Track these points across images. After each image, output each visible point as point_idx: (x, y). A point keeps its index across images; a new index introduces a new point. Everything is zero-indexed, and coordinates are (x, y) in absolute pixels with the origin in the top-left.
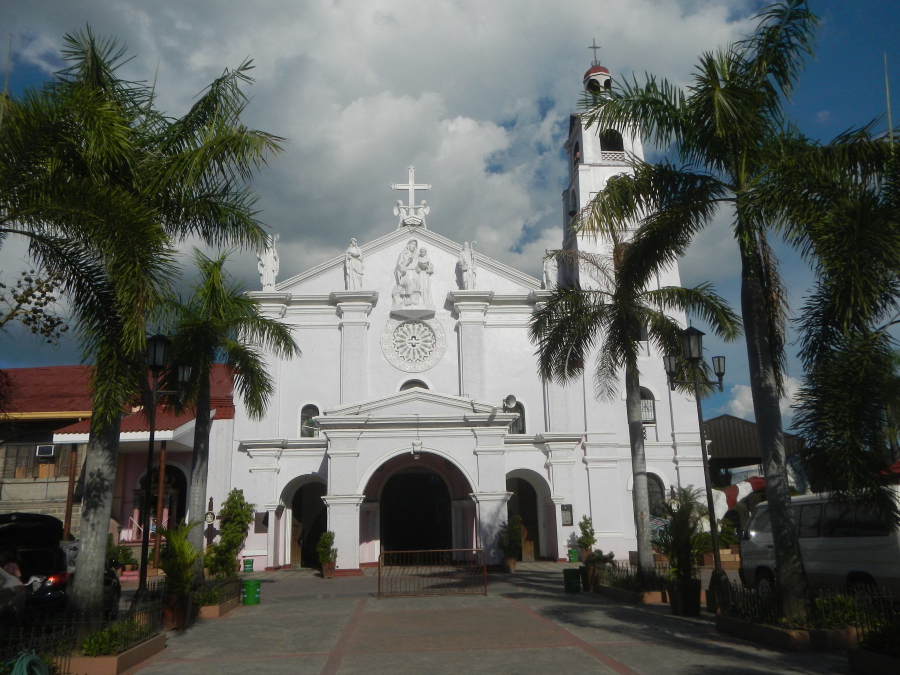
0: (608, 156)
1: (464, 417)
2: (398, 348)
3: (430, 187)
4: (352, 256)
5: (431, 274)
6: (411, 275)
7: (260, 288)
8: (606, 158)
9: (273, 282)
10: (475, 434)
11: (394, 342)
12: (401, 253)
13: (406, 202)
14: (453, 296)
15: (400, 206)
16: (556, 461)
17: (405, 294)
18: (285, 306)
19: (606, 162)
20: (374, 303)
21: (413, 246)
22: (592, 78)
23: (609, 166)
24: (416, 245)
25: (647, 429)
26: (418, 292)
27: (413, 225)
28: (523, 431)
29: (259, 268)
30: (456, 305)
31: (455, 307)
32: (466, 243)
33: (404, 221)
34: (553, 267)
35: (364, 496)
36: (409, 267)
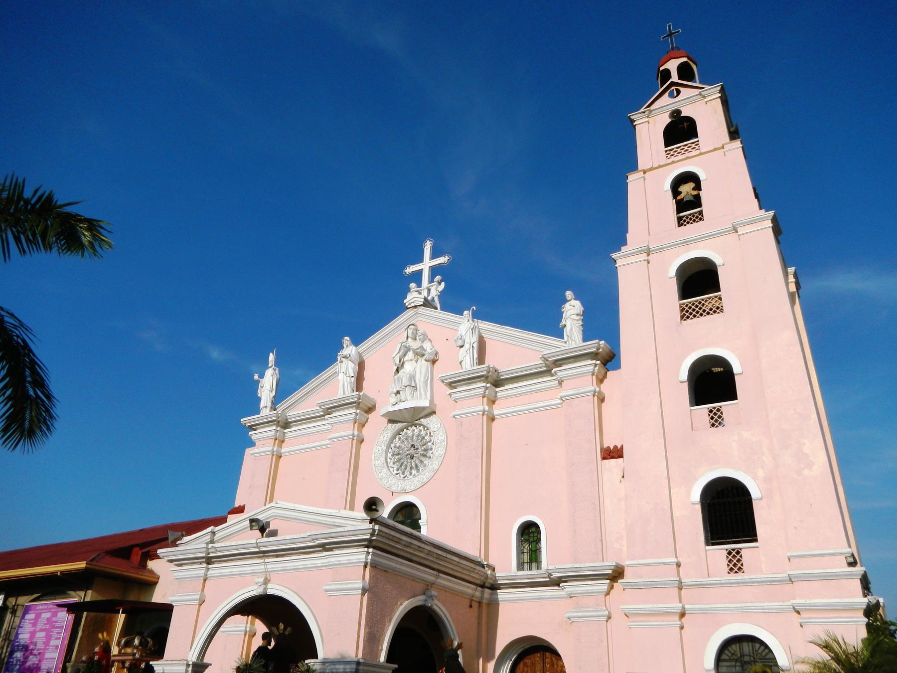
0: (675, 151)
2: (394, 464)
3: (447, 258)
4: (343, 357)
5: (434, 362)
6: (408, 367)
8: (672, 155)
9: (269, 404)
11: (390, 455)
13: (419, 285)
16: (575, 614)
17: (395, 391)
18: (279, 429)
19: (673, 159)
20: (370, 410)
21: (410, 331)
22: (661, 69)
23: (673, 162)
25: (743, 552)
26: (408, 385)
27: (415, 307)
28: (539, 567)
34: (575, 317)
36: (406, 358)
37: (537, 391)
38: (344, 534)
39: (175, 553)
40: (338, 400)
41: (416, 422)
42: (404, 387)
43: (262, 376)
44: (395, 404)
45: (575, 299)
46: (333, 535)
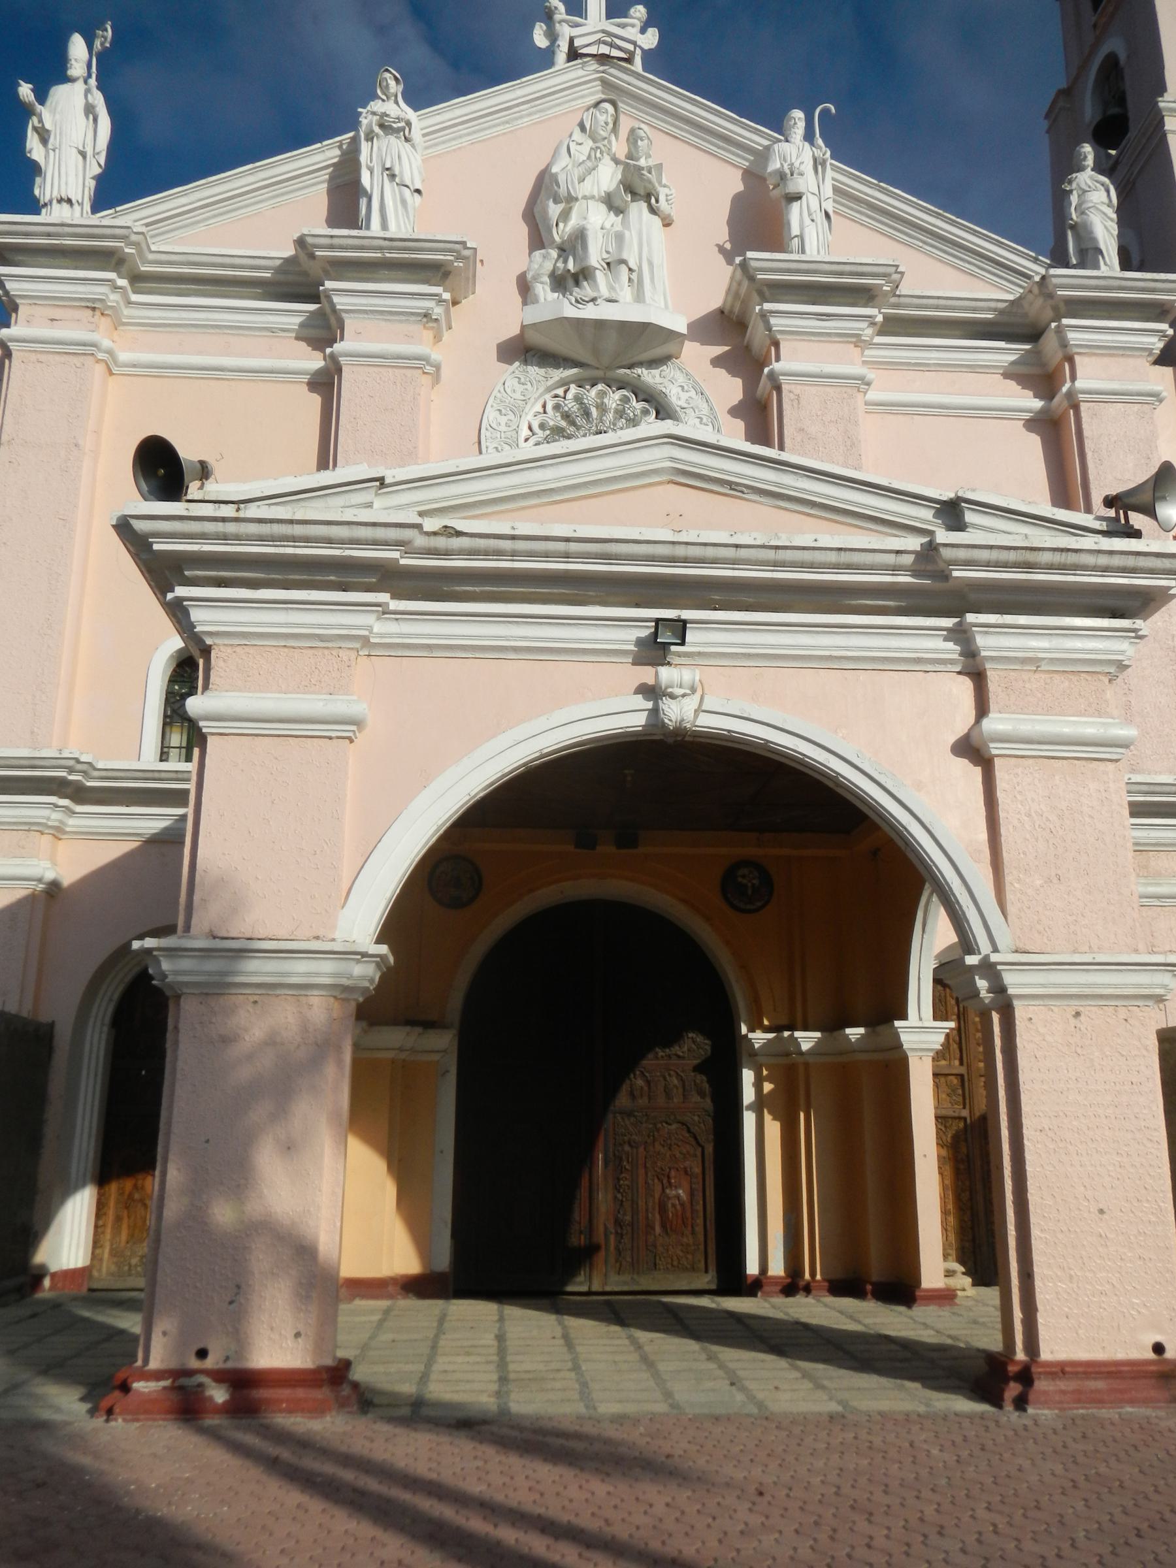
1: (931, 550)
4: (382, 126)
7: (34, 206)
10: (970, 653)
12: (561, 142)
14: (752, 279)
15: (557, 17)
18: (122, 282)
24: (616, 122)
27: (603, 59)
29: (33, 143)
30: (764, 315)
31: (757, 335)
32: (798, 115)
33: (571, 40)
35: (384, 949)
37: (973, 368)
38: (1090, 560)
39: (231, 528)
40: (387, 243)
41: (622, 371)
42: (606, 266)
43: (42, 96)
44: (587, 302)
45: (1098, 168)
46: (1046, 557)
